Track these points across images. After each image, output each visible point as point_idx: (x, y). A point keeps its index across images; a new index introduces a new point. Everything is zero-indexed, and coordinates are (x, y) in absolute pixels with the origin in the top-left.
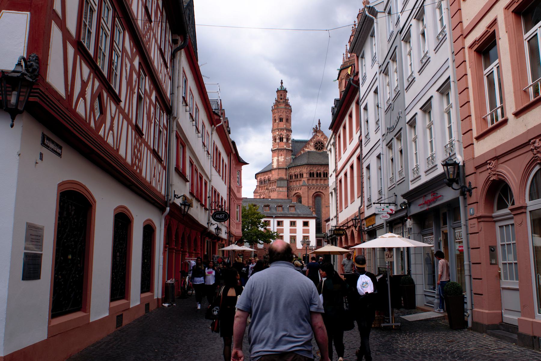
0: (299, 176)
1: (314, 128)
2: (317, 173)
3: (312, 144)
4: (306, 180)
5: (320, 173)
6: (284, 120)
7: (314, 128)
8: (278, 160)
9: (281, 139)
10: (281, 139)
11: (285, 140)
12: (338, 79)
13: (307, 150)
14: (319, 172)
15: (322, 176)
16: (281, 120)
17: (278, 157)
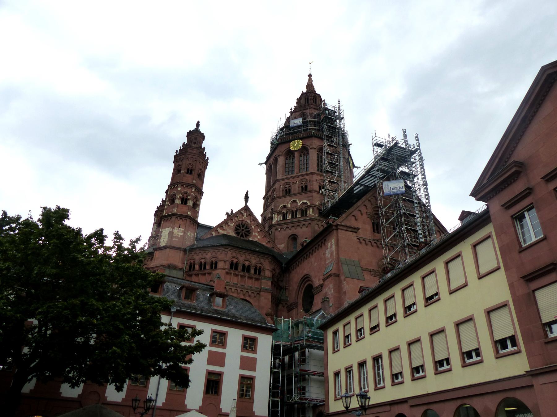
0: (208, 267)
1: (227, 213)
2: (244, 266)
3: (232, 225)
4: (222, 273)
5: (249, 267)
6: (195, 173)
7: (227, 213)
8: (171, 234)
9: (184, 201)
10: (184, 201)
11: (190, 203)
12: (266, 163)
13: (221, 231)
14: (247, 263)
15: (252, 271)
16: (190, 171)
17: (173, 228)
